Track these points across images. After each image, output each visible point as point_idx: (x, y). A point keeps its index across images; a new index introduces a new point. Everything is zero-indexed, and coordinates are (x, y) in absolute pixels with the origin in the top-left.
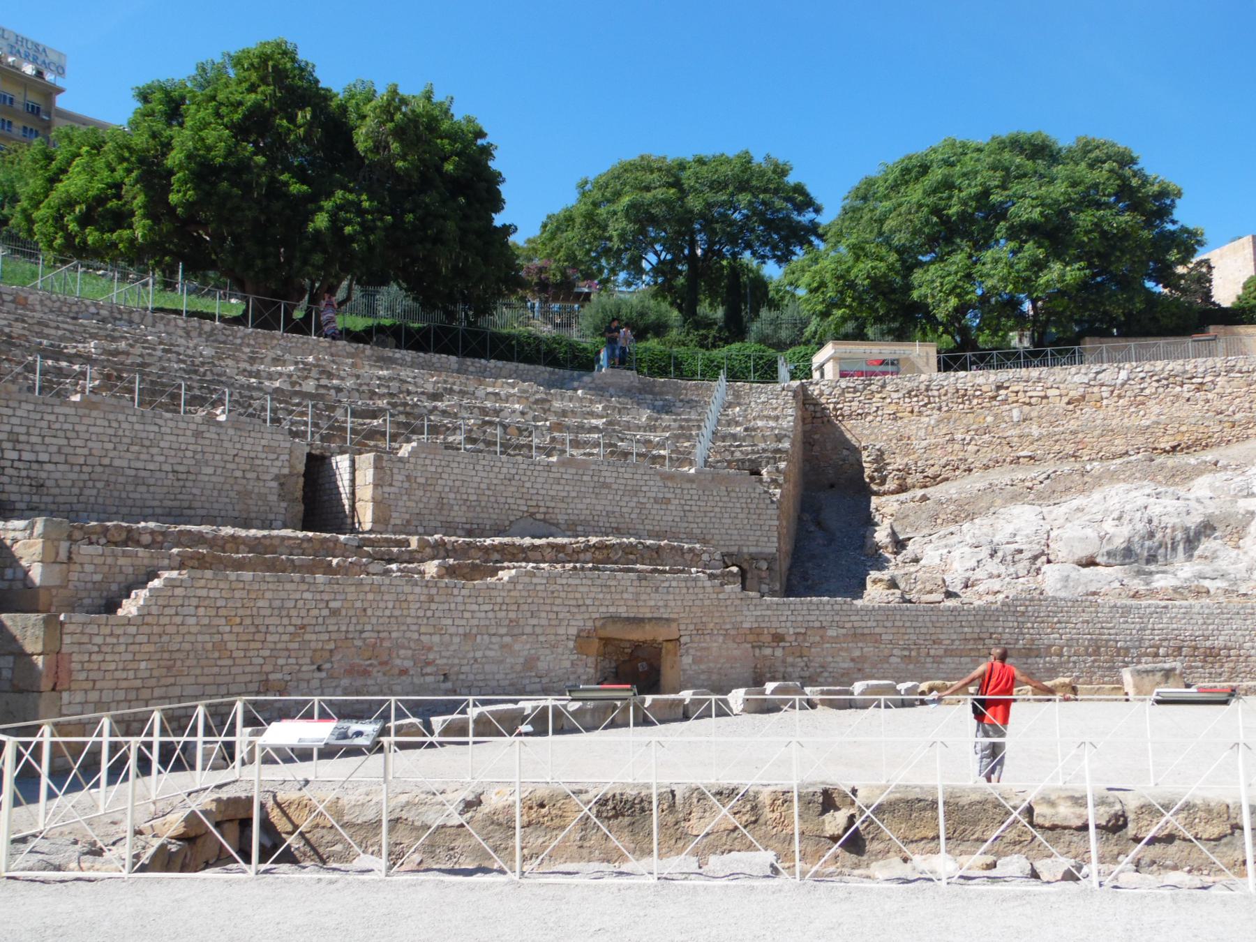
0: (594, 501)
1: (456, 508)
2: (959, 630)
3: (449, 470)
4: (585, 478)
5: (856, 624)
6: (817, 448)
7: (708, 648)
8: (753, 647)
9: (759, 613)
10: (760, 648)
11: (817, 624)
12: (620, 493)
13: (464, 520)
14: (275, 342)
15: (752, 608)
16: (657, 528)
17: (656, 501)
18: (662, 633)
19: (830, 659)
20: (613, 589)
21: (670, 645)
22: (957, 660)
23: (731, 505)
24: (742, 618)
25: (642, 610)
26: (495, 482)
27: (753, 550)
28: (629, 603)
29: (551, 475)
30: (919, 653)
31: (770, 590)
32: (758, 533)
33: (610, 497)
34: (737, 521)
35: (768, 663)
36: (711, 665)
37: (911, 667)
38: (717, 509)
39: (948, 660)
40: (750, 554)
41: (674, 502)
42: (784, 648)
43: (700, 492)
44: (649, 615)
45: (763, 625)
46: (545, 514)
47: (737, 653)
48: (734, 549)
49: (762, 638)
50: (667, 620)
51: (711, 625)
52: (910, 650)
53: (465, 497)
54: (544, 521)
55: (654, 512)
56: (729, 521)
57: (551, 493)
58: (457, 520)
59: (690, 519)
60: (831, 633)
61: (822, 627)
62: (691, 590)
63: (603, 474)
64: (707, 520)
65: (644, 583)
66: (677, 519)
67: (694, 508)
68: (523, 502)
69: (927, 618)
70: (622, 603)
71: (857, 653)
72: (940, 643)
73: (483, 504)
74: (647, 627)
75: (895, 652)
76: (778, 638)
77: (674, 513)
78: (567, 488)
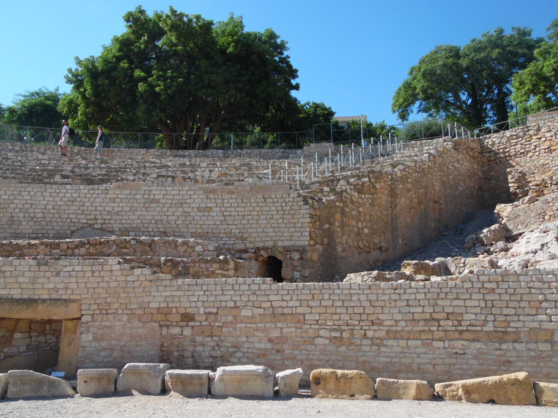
0: (144, 213)
1: (24, 223)
2: (406, 310)
3: (21, 197)
4: (137, 197)
5: (275, 304)
6: (493, 181)
7: (111, 327)
8: (161, 326)
9: (169, 294)
10: (168, 326)
11: (232, 304)
12: (168, 205)
13: (31, 231)
14: (114, 154)
15: (161, 289)
16: (200, 231)
17: (199, 209)
18: (57, 313)
19: (244, 339)
20: (8, 274)
21: (70, 324)
22: (403, 343)
23: (267, 209)
24: (151, 299)
25: (37, 292)
26: (59, 203)
27: (287, 243)
28: (24, 286)
29: (108, 196)
30: (352, 335)
31: (302, 276)
32: (292, 230)
33: (157, 209)
34: (272, 221)
35: (176, 342)
36: (114, 342)
37: (343, 349)
38: (255, 213)
39: (390, 343)
40: (284, 248)
41: (214, 209)
42: (193, 327)
43: (239, 201)
44: (46, 297)
45: (170, 305)
46: (102, 224)
47: (142, 331)
48: (270, 244)
49: (170, 318)
50: (65, 300)
51: (116, 305)
52: (342, 331)
53: (32, 215)
54: (102, 229)
55: (197, 218)
56: (266, 221)
57: (107, 209)
58: (24, 231)
59: (229, 222)
60: (245, 312)
61: (236, 307)
62: (96, 274)
63: (153, 192)
64: (244, 222)
65: (43, 268)
66: (219, 223)
67: (233, 213)
68: (83, 216)
69: (363, 298)
70: (17, 286)
71: (275, 334)
72: (381, 324)
73: (48, 219)
74: (40, 307)
75: (322, 333)
76: (187, 318)
77: (215, 218)
78: (121, 205)
